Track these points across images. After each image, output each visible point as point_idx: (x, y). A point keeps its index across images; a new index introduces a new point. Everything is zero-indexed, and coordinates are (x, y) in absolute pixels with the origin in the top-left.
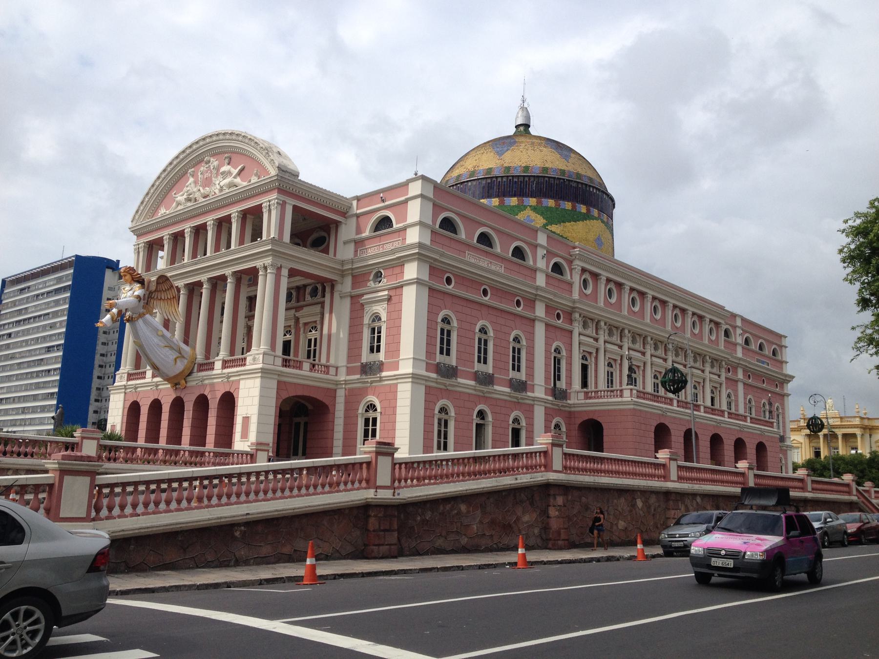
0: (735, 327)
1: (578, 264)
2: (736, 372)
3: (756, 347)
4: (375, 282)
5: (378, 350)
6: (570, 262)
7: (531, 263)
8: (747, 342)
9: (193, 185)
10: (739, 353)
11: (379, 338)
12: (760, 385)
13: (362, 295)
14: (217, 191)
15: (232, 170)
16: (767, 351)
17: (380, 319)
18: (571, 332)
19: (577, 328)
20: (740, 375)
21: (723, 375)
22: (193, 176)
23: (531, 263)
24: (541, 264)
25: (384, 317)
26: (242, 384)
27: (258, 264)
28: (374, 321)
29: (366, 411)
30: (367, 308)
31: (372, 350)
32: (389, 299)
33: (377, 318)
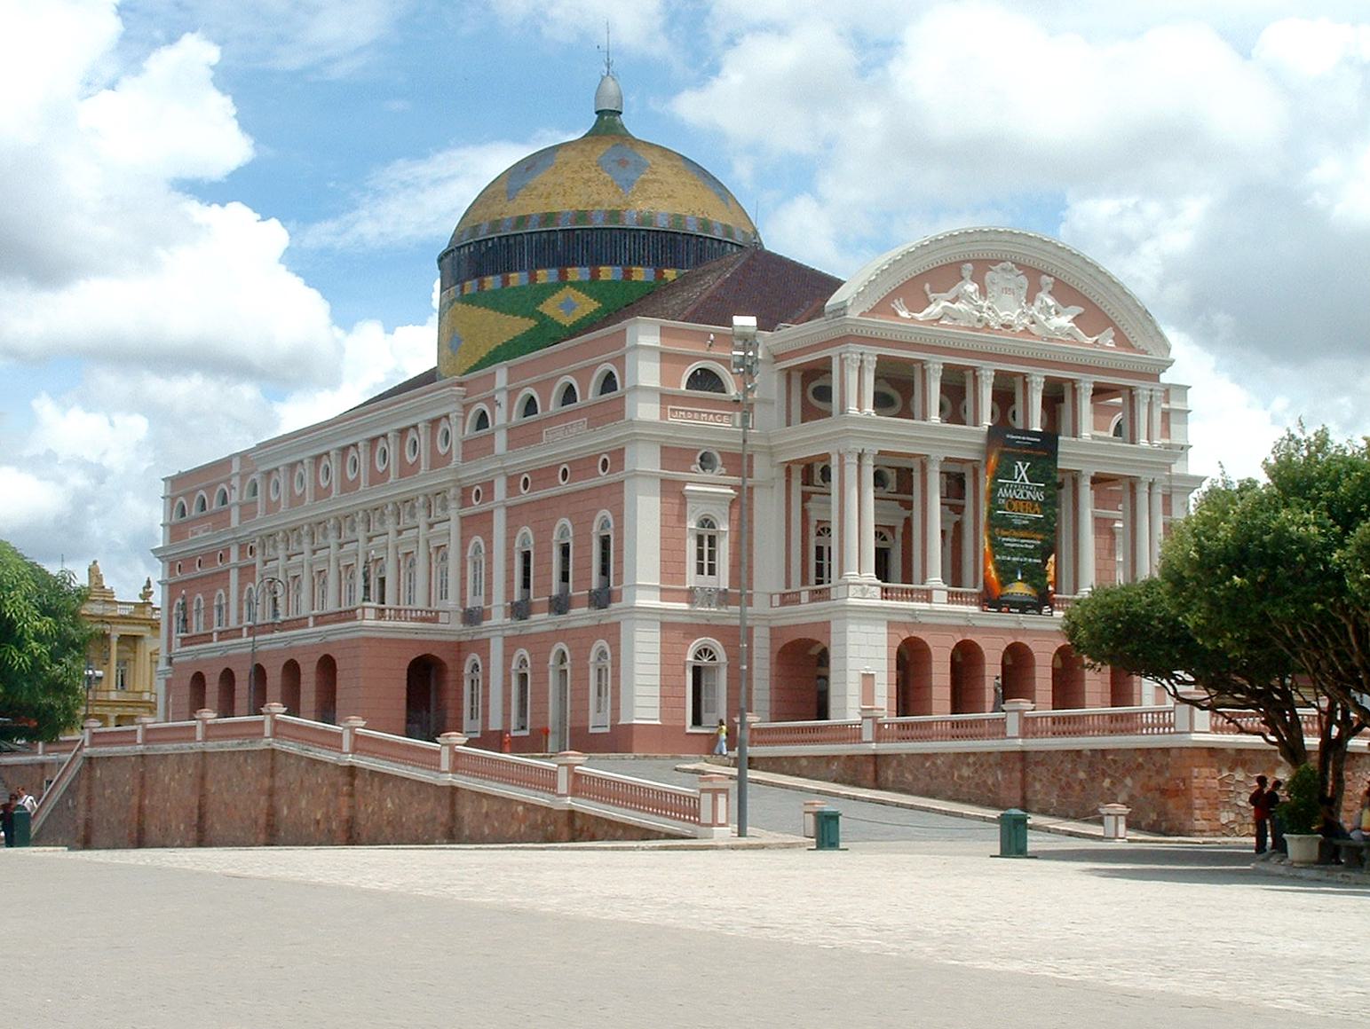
27: (1146, 476)
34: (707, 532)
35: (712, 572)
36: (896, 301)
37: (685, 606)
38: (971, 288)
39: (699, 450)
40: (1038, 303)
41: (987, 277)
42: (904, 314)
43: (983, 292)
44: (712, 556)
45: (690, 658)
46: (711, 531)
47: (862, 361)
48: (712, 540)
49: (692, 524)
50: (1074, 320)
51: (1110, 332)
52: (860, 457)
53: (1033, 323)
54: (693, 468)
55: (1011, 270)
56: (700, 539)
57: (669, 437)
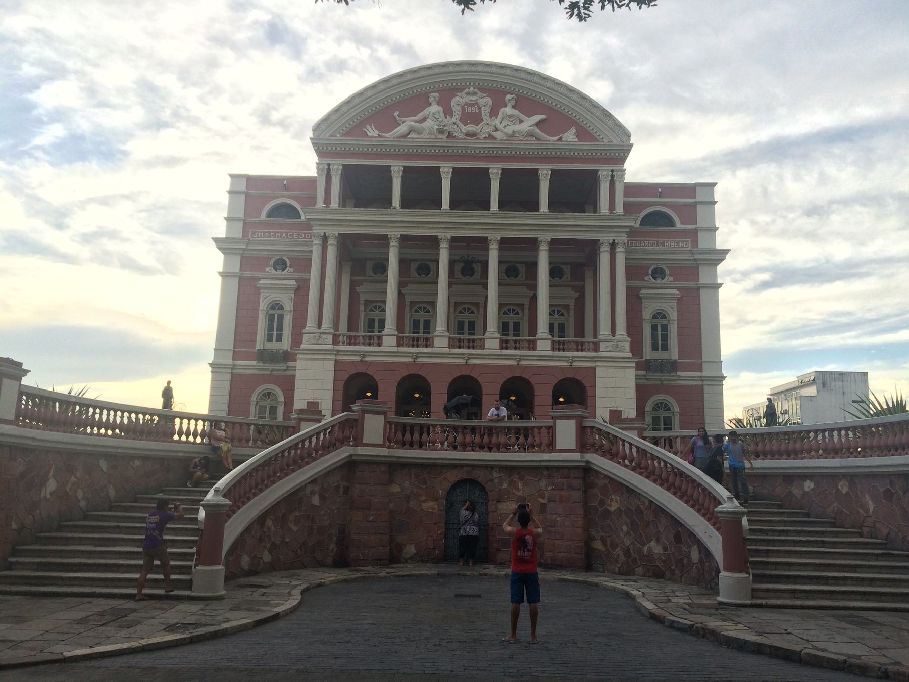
4: (655, 279)
5: (665, 347)
9: (442, 114)
11: (665, 337)
13: (640, 289)
14: (497, 135)
15: (522, 116)
17: (664, 317)
22: (438, 104)
25: (673, 315)
26: (599, 372)
27: (606, 238)
28: (654, 317)
29: (654, 409)
30: (645, 303)
31: (655, 347)
32: (679, 299)
33: (660, 315)
34: (276, 313)
35: (279, 338)
36: (368, 127)
37: (254, 363)
38: (434, 108)
39: (270, 258)
40: (500, 116)
41: (453, 103)
42: (377, 132)
43: (448, 112)
44: (280, 328)
45: (254, 398)
46: (280, 312)
47: (329, 170)
48: (281, 318)
49: (263, 306)
50: (538, 124)
51: (573, 130)
52: (325, 239)
53: (497, 130)
54: (267, 269)
55: (475, 94)
56: (271, 318)
57: (244, 250)
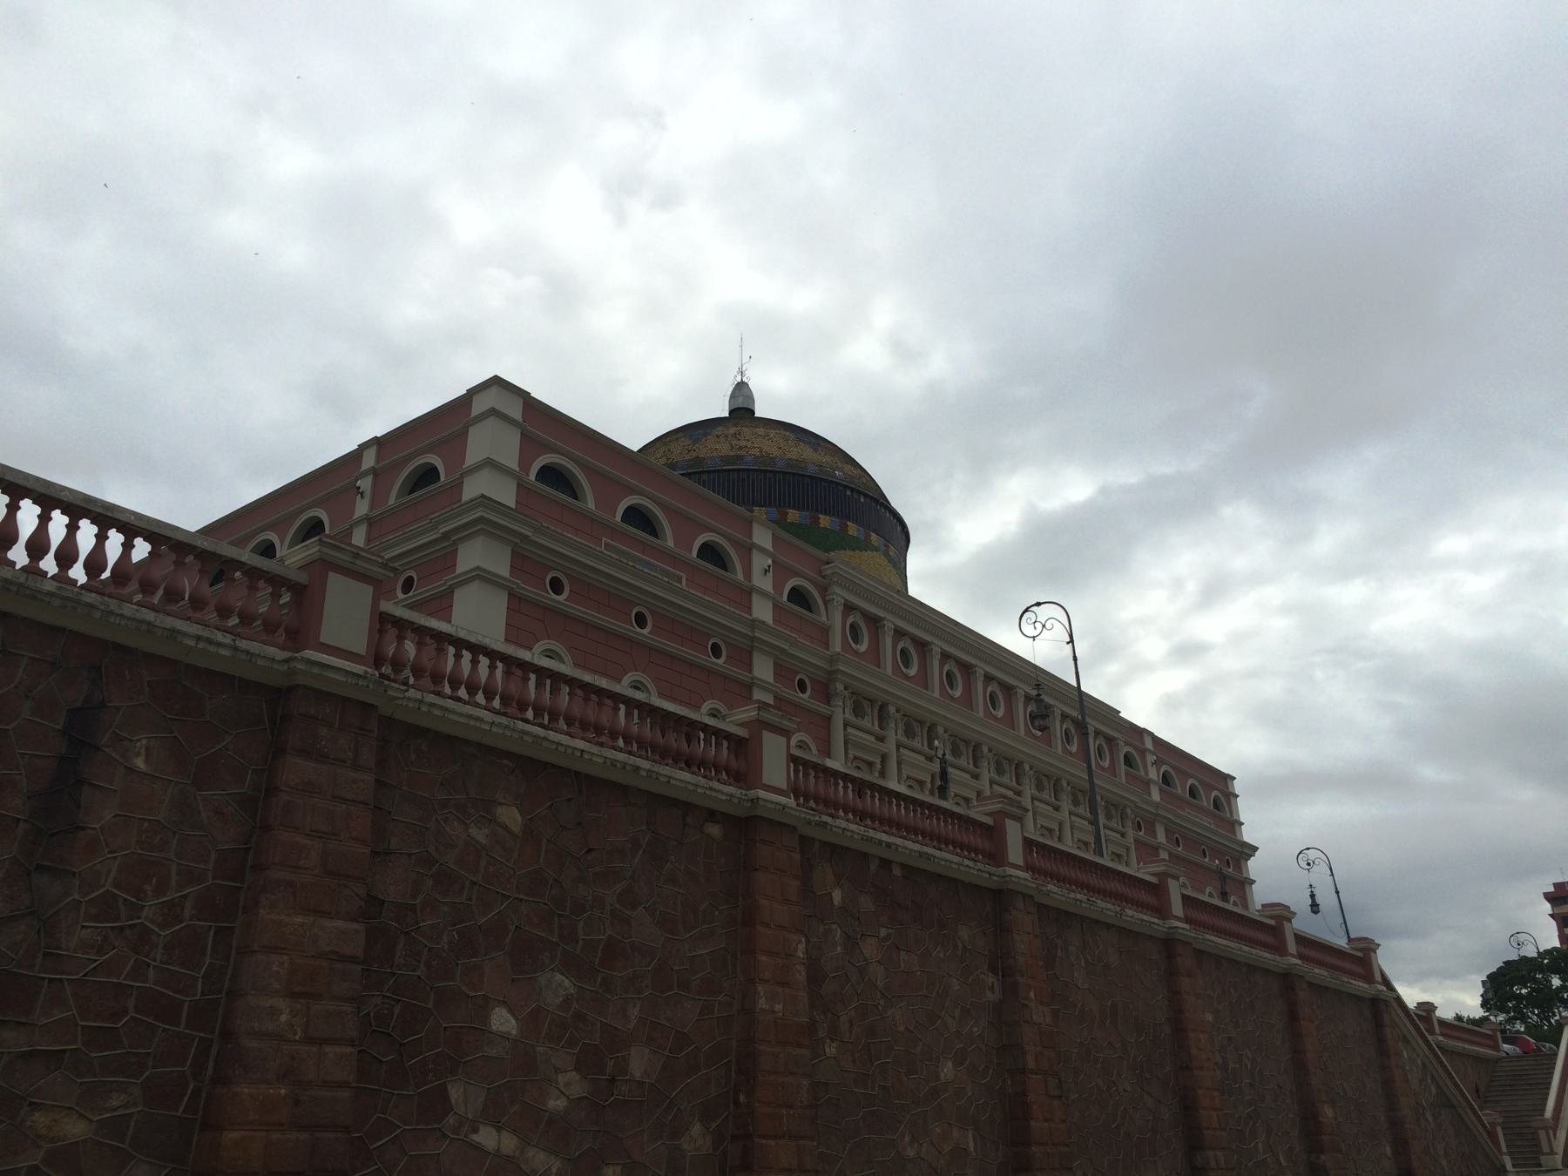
0: (1143, 752)
1: (839, 594)
2: (1154, 834)
3: (1184, 791)
6: (824, 590)
7: (740, 576)
8: (1166, 779)
10: (1156, 796)
12: (1196, 858)
16: (1206, 802)
18: (829, 719)
19: (840, 713)
20: (1161, 837)
21: (1131, 833)
23: (740, 576)
24: (765, 583)
